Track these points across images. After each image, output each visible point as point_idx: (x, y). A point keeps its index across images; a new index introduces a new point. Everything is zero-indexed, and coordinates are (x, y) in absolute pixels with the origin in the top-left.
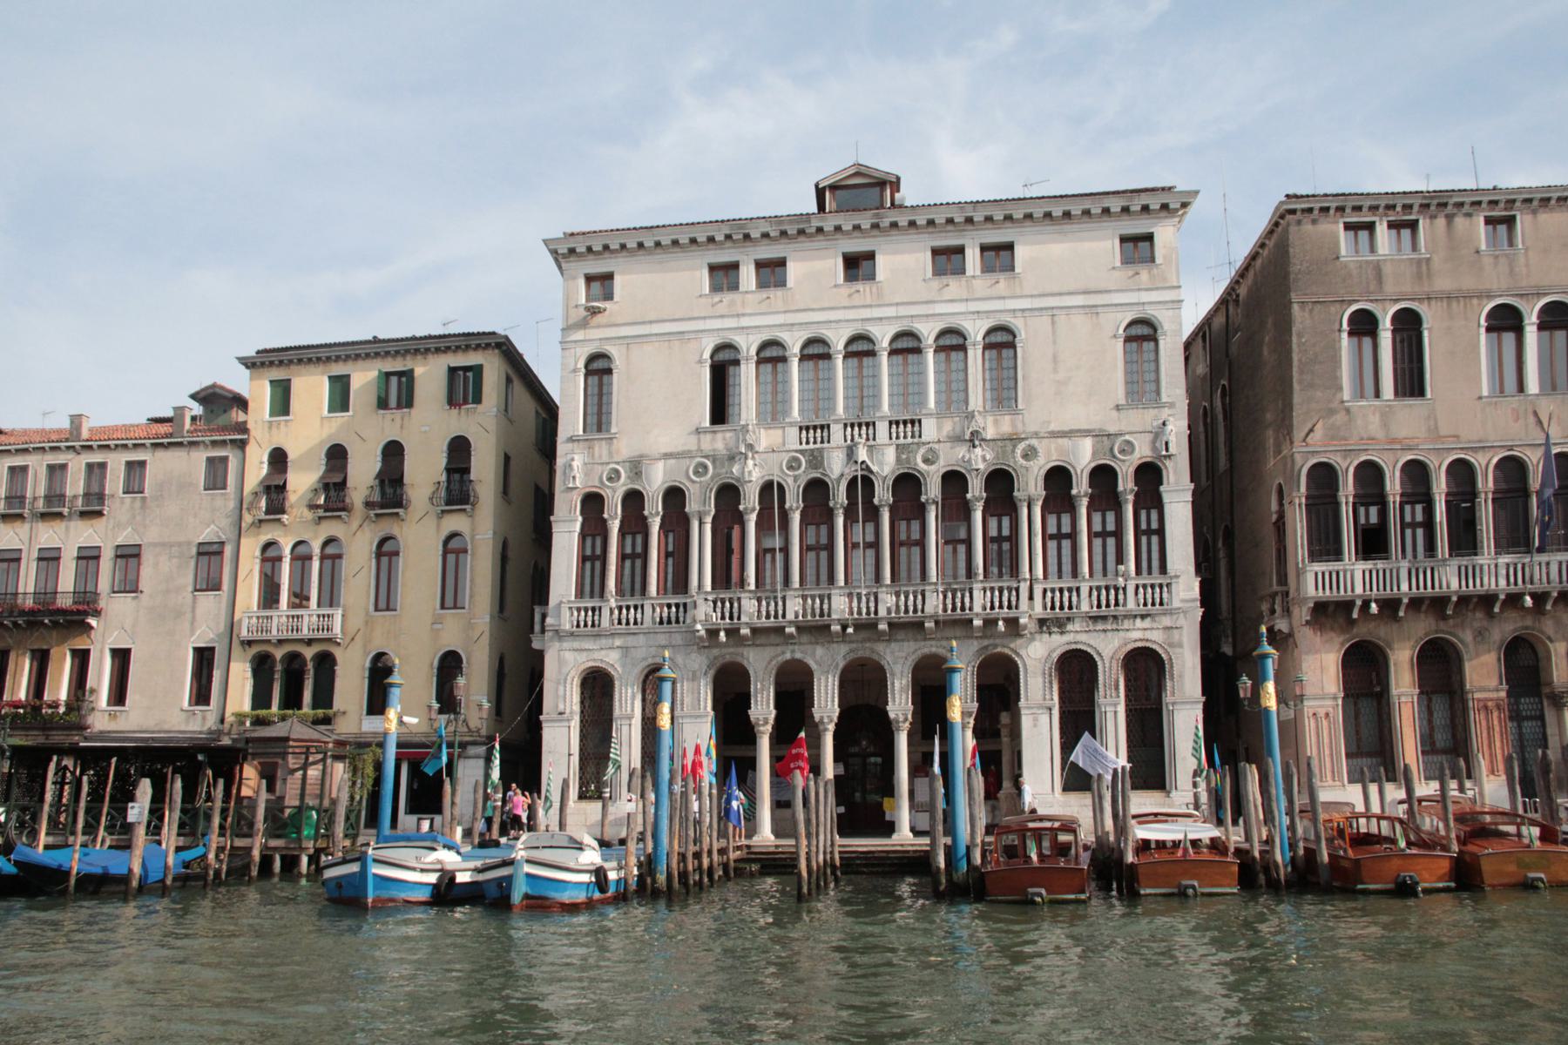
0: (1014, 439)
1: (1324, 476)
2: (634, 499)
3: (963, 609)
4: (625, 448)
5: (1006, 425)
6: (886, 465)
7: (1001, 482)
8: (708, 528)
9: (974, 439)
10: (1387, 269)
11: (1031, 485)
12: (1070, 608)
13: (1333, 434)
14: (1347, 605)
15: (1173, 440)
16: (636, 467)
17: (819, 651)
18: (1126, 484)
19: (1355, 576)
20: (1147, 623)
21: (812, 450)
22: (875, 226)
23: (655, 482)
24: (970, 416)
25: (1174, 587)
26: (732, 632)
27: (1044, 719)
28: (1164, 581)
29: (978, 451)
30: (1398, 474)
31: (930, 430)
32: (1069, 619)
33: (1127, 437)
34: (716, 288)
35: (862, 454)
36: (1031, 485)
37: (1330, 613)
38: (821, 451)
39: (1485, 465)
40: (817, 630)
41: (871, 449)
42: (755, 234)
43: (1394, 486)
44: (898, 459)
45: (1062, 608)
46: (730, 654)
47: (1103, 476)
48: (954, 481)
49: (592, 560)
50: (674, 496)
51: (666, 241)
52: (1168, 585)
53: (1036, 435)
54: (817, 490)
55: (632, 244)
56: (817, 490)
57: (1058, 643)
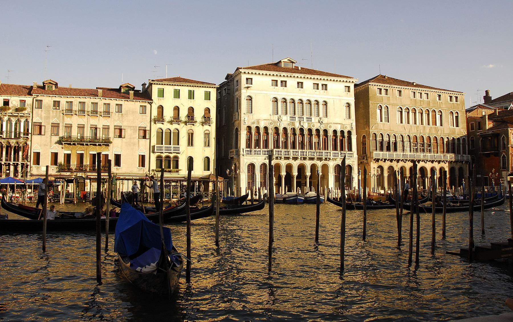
0: (328, 124)
2: (258, 128)
7: (326, 131)
10: (384, 98)
11: (330, 134)
13: (376, 128)
16: (258, 121)
18: (346, 134)
23: (262, 126)
35: (302, 124)
47: (342, 132)
48: (318, 131)
50: (266, 128)
54: (294, 130)
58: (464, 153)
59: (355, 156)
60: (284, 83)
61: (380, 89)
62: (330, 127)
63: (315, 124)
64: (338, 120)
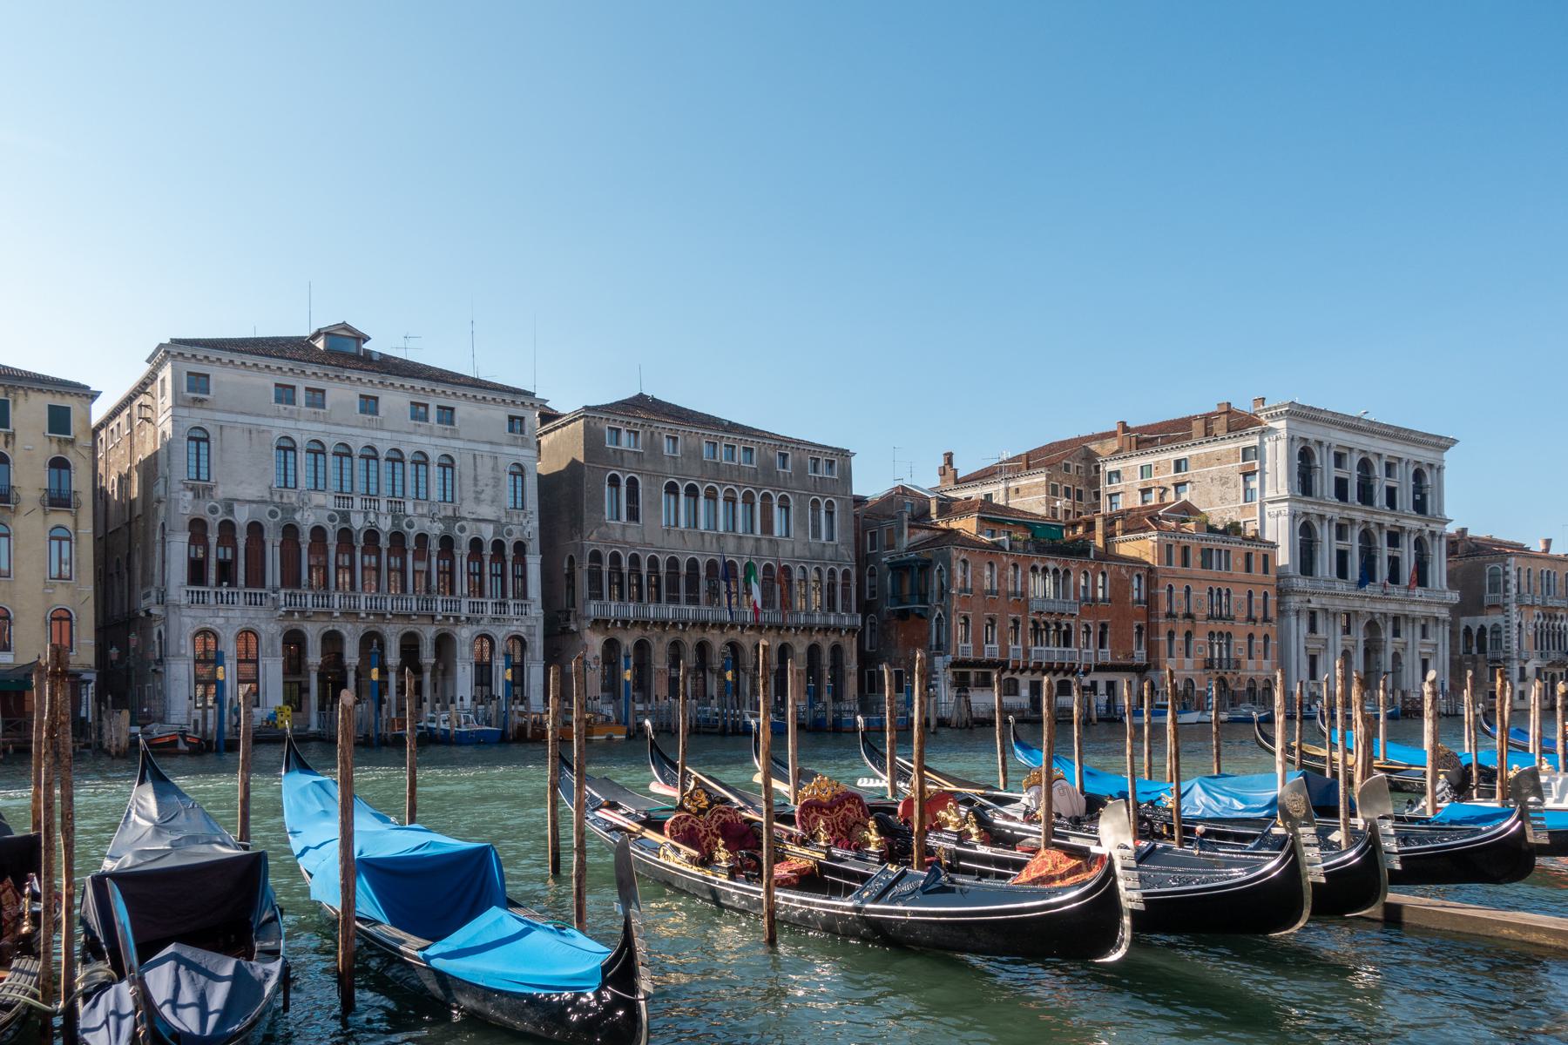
0: (455, 518)
6: (385, 525)
8: (277, 550)
13: (602, 538)
14: (607, 622)
16: (229, 505)
17: (349, 626)
19: (613, 609)
23: (242, 517)
34: (278, 400)
35: (372, 517)
37: (600, 624)
38: (348, 513)
39: (663, 559)
41: (377, 516)
47: (498, 546)
48: (422, 538)
53: (465, 519)
54: (346, 535)
57: (476, 629)
58: (846, 608)
59: (536, 610)
60: (317, 397)
61: (618, 431)
63: (415, 520)
64: (487, 511)
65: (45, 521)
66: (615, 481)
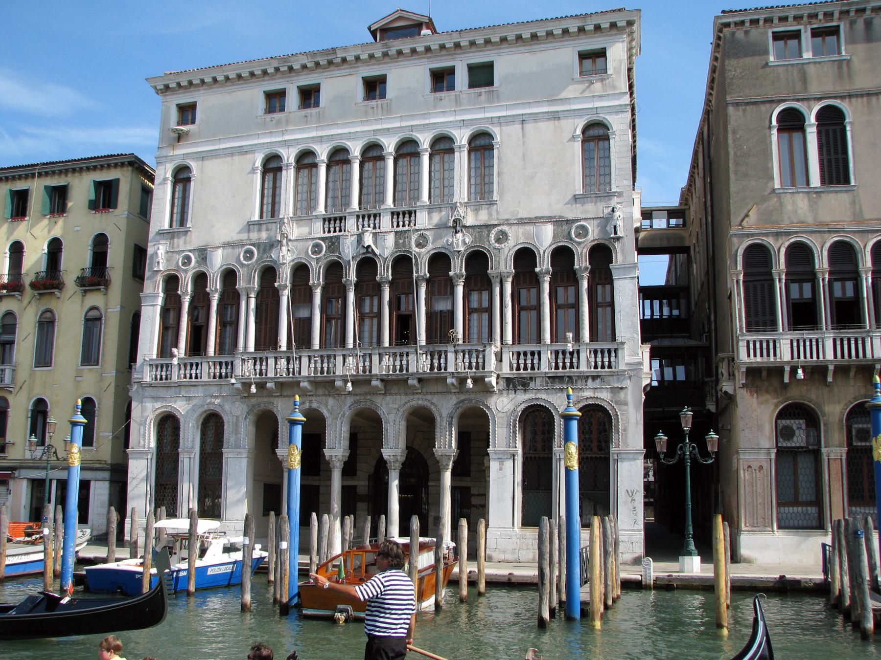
0: (489, 227)
1: (758, 256)
2: (201, 279)
3: (439, 368)
4: (195, 239)
5: (483, 217)
7: (478, 260)
8: (253, 302)
9: (457, 226)
11: (503, 264)
12: (533, 368)
15: (620, 223)
17: (331, 401)
18: (582, 262)
20: (597, 384)
21: (331, 238)
22: (385, 54)
24: (453, 207)
25: (620, 352)
26: (261, 386)
27: (509, 464)
28: (612, 346)
29: (459, 235)
30: (825, 253)
31: (423, 220)
32: (531, 378)
33: (582, 223)
34: (270, 110)
35: (368, 240)
36: (503, 264)
40: (325, 385)
41: (375, 235)
42: (296, 66)
43: (822, 263)
44: (397, 244)
45: (525, 368)
46: (263, 403)
49: (169, 330)
50: (229, 276)
51: (232, 75)
52: (616, 350)
55: (208, 79)
56: (335, 269)
62: (502, 237)
65: (83, 301)
66: (792, 122)
